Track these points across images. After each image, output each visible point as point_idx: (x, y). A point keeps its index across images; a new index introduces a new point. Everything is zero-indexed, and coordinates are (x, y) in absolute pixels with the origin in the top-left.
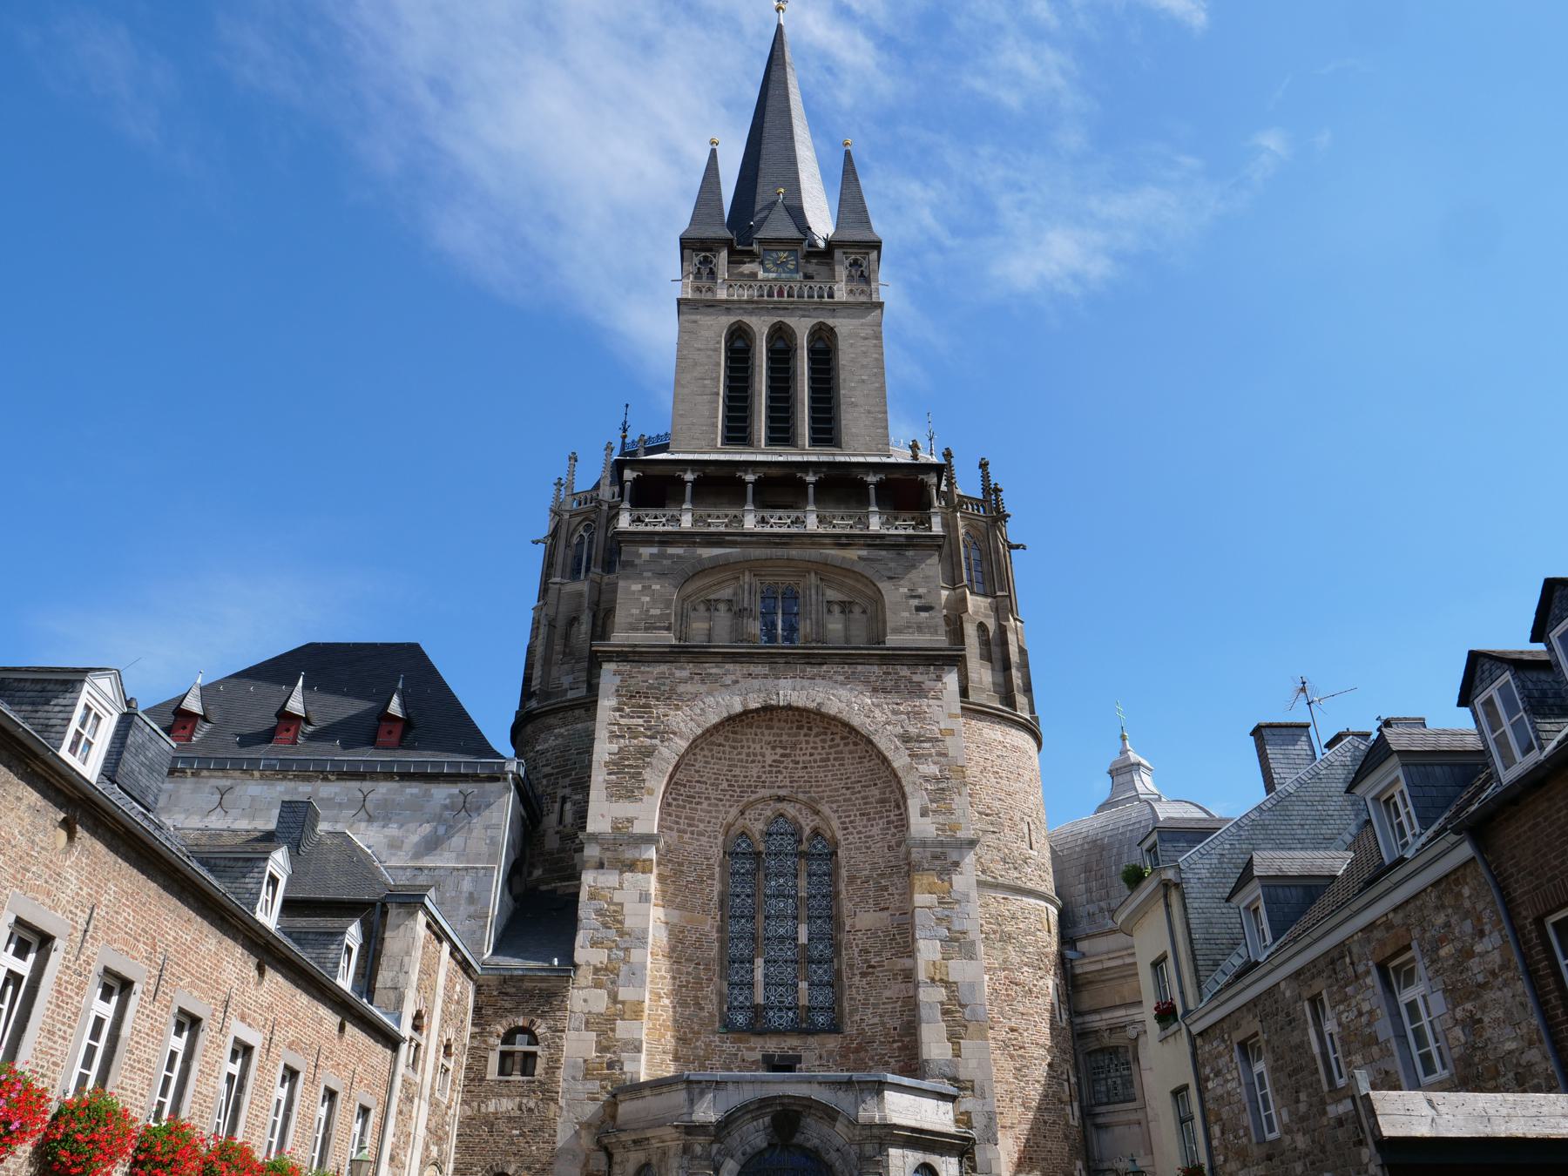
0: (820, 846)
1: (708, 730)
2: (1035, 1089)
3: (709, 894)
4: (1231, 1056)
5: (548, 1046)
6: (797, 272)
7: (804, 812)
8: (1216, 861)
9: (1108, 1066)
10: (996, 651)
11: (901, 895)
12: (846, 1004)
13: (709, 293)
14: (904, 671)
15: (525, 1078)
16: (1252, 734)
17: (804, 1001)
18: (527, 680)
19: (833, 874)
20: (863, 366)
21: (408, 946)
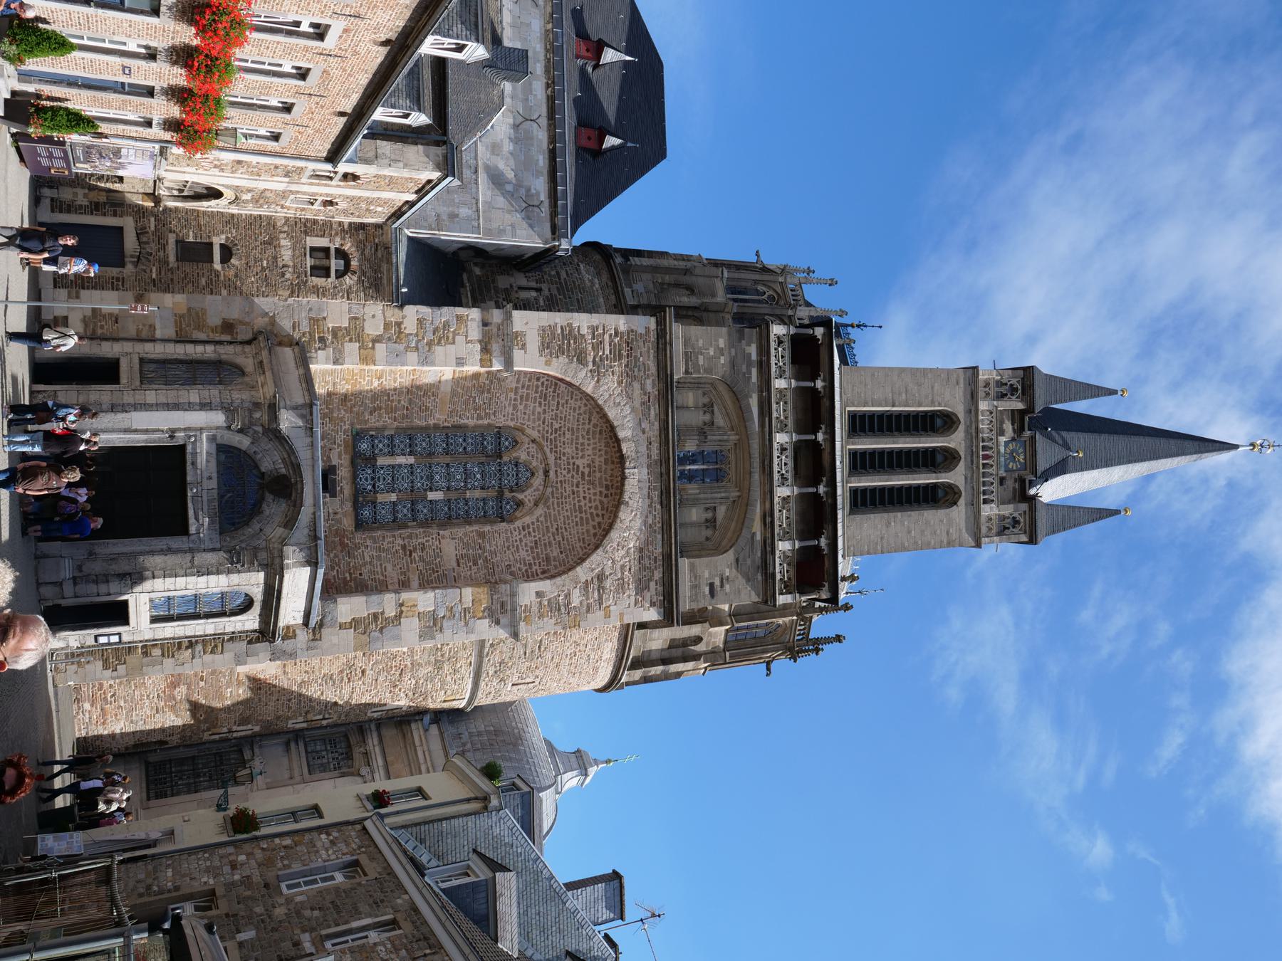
0: (508, 507)
1: (602, 409)
2: (316, 692)
3: (465, 415)
4: (347, 854)
5: (335, 287)
6: (1006, 471)
7: (536, 493)
8: (507, 841)
9: (336, 752)
10: (677, 652)
11: (471, 576)
12: (379, 533)
13: (984, 394)
14: (658, 575)
15: (309, 269)
16: (614, 871)
17: (381, 498)
18: (638, 253)
19: (486, 519)
20: (923, 532)
21: (411, 165)
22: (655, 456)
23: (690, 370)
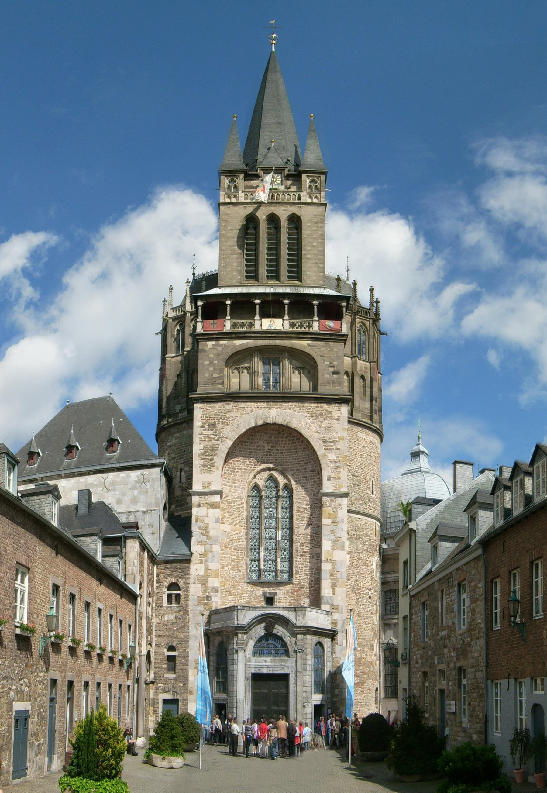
23: (221, 382)
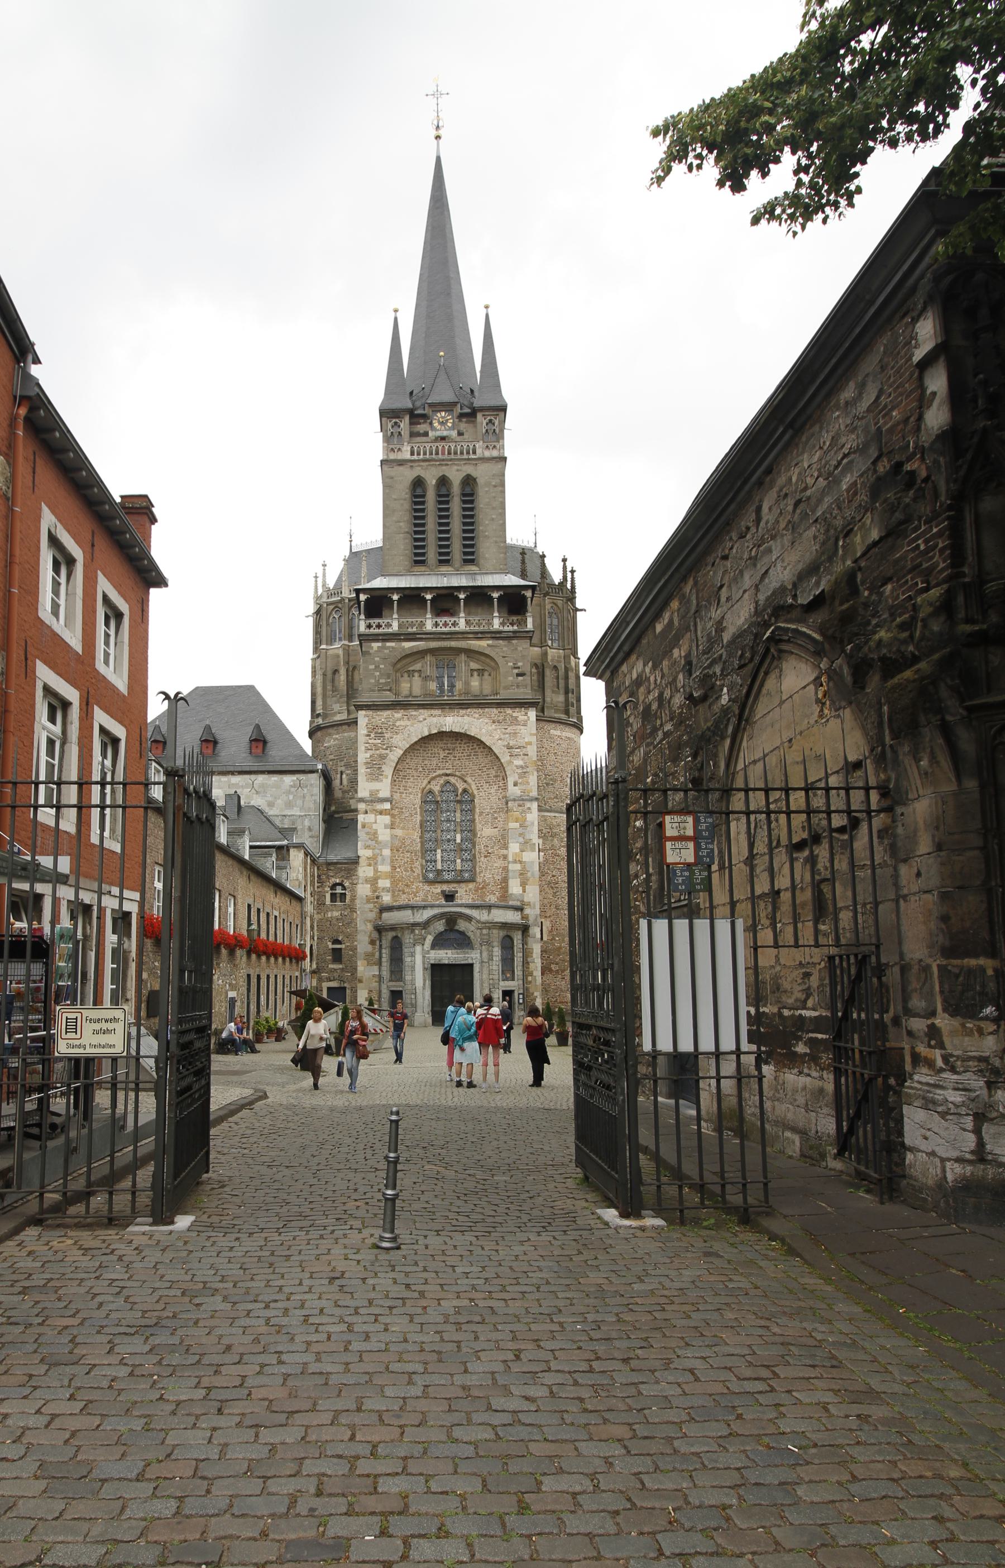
1: (413, 745)
14: (509, 711)
17: (459, 868)
19: (472, 811)
20: (494, 508)
22: (438, 712)
